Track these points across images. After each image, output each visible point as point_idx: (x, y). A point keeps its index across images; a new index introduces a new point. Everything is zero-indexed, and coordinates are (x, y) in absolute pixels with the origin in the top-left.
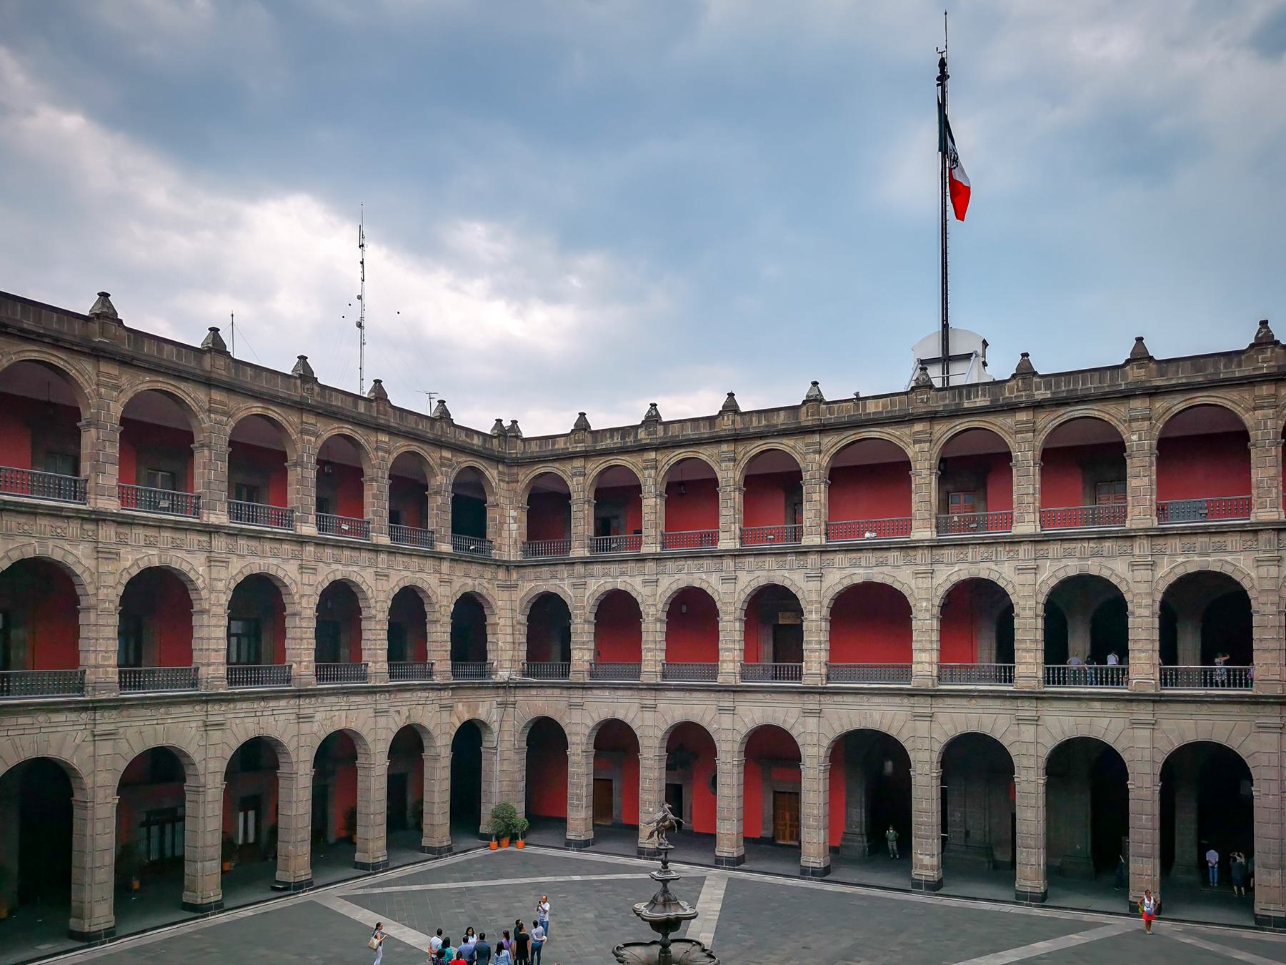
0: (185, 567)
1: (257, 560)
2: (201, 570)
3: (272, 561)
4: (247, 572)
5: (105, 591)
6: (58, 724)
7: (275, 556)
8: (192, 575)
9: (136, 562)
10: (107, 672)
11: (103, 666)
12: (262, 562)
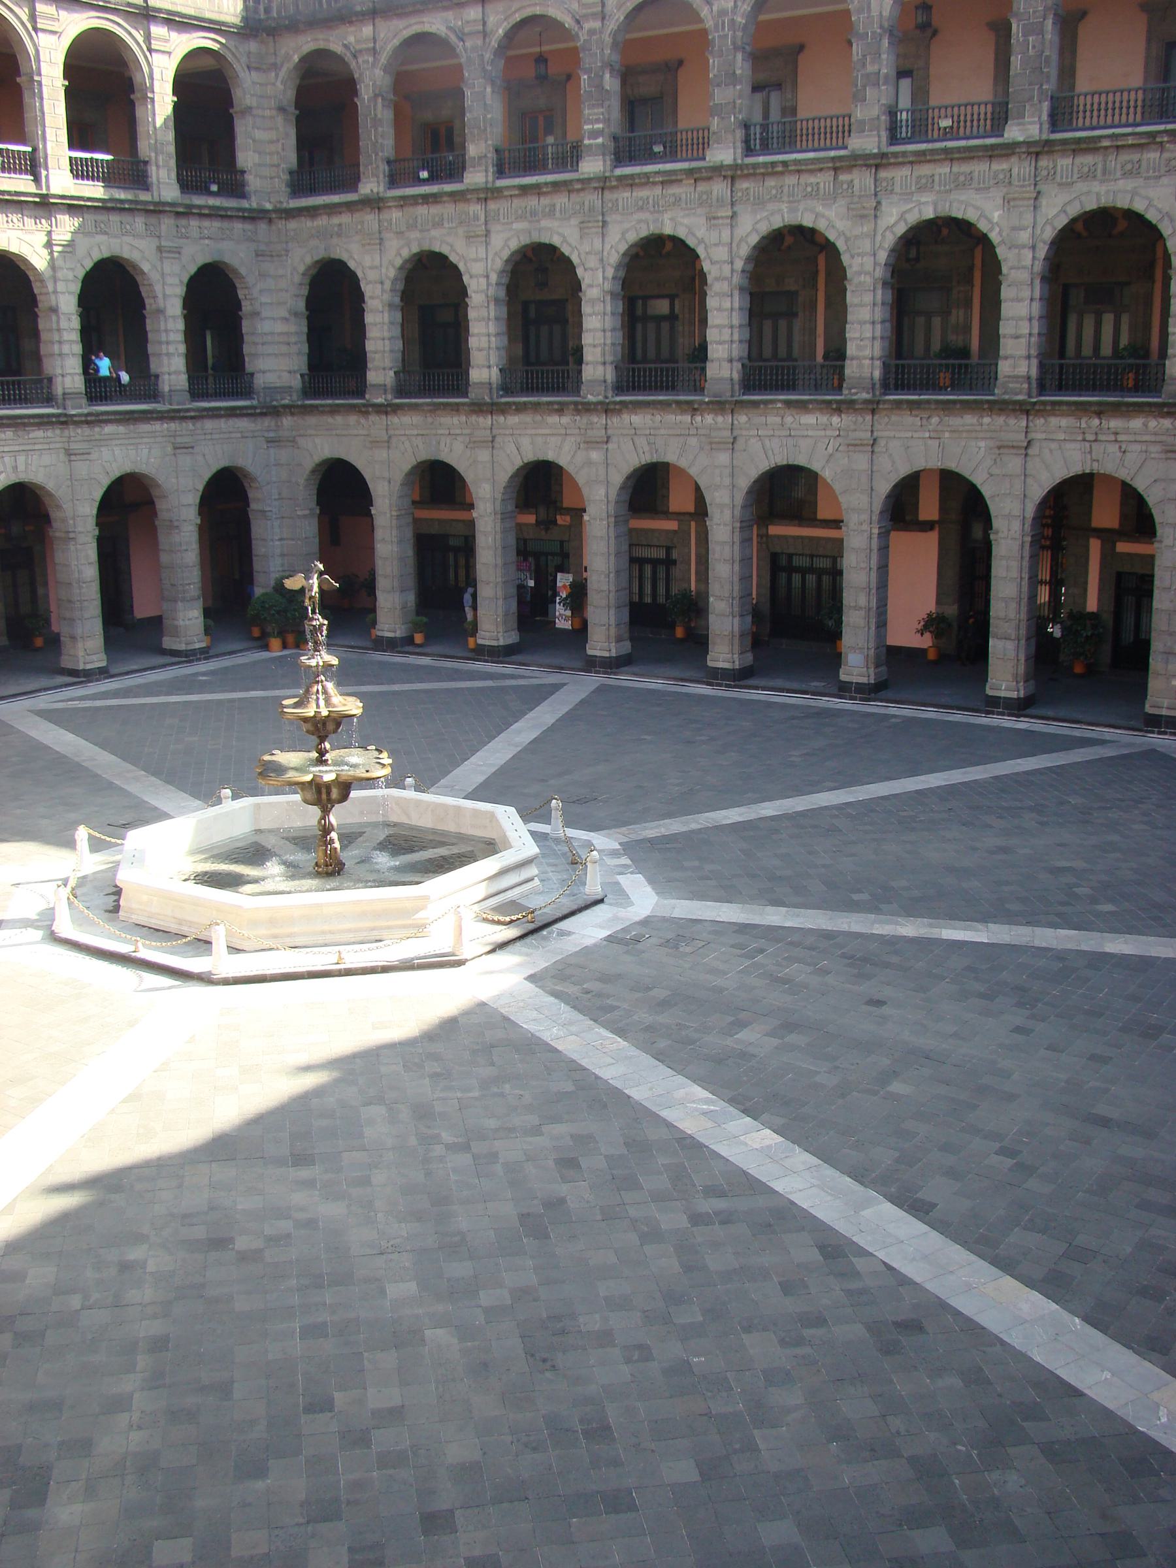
0: (971, 216)
1: (1096, 187)
2: (996, 216)
3: (1127, 184)
4: (1074, 211)
5: (858, 260)
6: (808, 427)
7: (1127, 174)
8: (983, 226)
9: (902, 217)
10: (860, 366)
11: (857, 358)
12: (1103, 189)
